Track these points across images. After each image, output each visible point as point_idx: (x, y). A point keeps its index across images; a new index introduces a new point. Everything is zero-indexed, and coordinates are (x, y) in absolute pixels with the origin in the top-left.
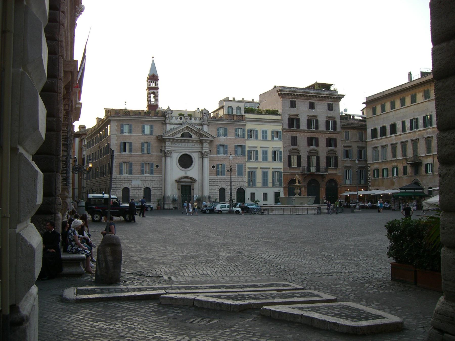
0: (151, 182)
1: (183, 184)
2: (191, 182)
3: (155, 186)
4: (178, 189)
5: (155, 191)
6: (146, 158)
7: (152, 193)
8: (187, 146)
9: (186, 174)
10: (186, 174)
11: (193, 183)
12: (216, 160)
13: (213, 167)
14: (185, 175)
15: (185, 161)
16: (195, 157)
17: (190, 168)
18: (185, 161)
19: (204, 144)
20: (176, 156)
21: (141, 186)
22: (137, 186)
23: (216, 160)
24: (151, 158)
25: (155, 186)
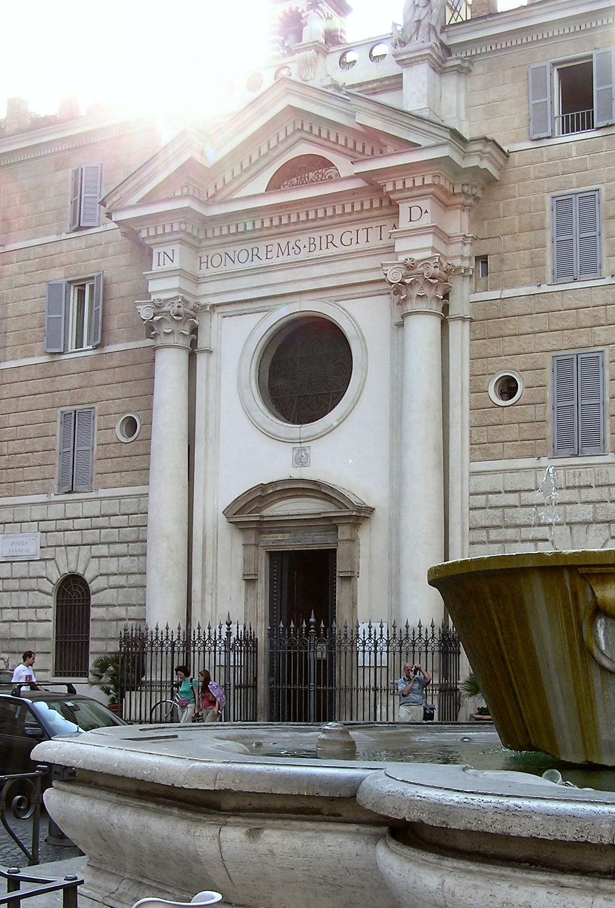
0: (90, 536)
1: (287, 542)
2: (330, 524)
3: (113, 565)
4: (250, 581)
5: (109, 596)
6: (74, 381)
7: (95, 613)
8: (304, 255)
9: (301, 461)
10: (301, 461)
11: (344, 532)
12: (526, 325)
13: (508, 388)
14: (297, 473)
15: (306, 370)
16: (363, 321)
17: (331, 418)
18: (306, 370)
19: (404, 209)
20: (236, 346)
21: (38, 568)
22: (20, 569)
23: (526, 325)
24: (99, 377)
25: (113, 565)
